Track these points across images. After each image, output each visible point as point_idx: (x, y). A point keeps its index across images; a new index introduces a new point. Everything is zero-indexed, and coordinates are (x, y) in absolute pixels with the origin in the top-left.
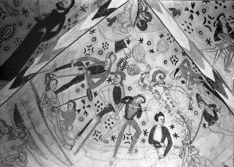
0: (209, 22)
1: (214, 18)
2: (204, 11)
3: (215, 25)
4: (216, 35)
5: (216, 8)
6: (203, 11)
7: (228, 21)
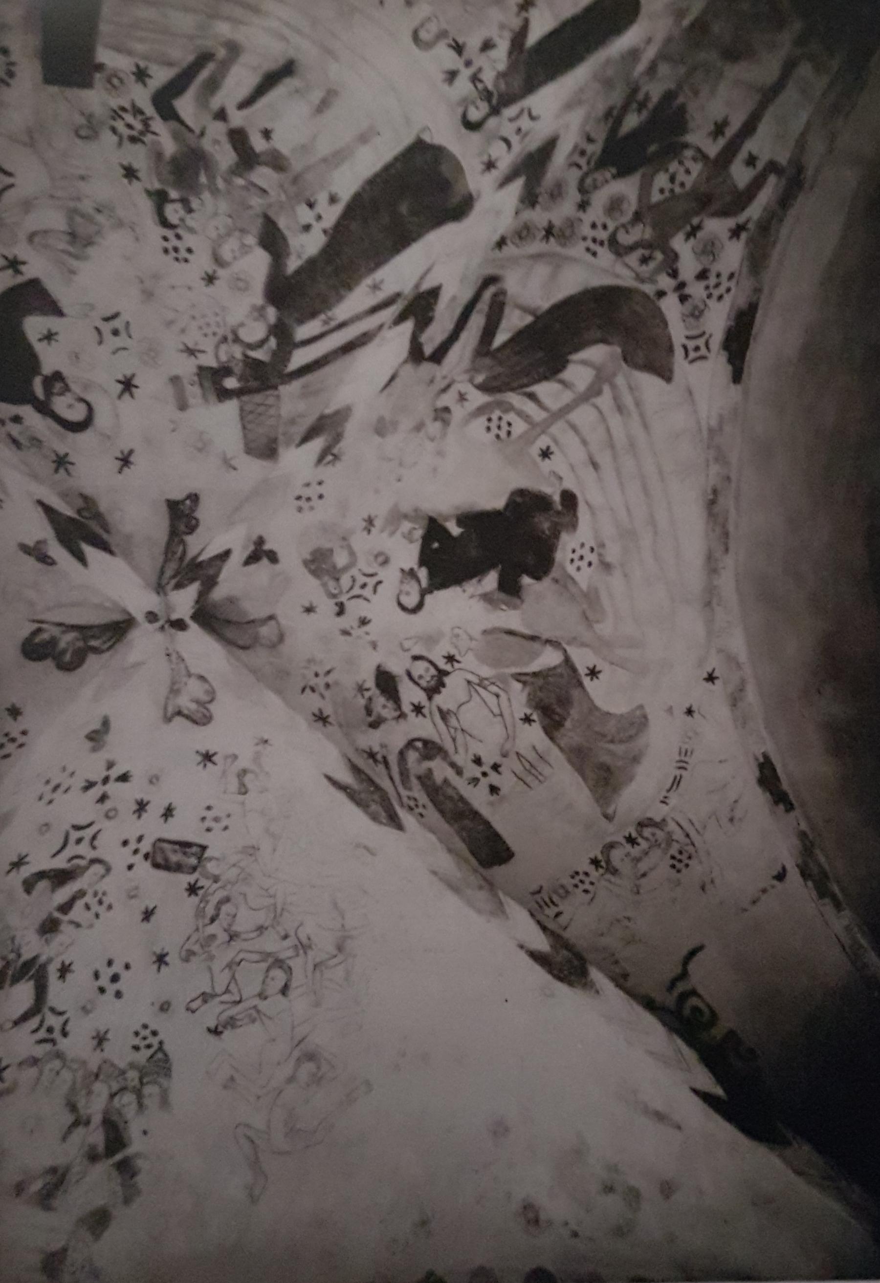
0: (79, 841)
1: (94, 848)
2: (111, 814)
3: (76, 861)
4: (41, 875)
5: (125, 843)
6: (110, 810)
7: (90, 893)
